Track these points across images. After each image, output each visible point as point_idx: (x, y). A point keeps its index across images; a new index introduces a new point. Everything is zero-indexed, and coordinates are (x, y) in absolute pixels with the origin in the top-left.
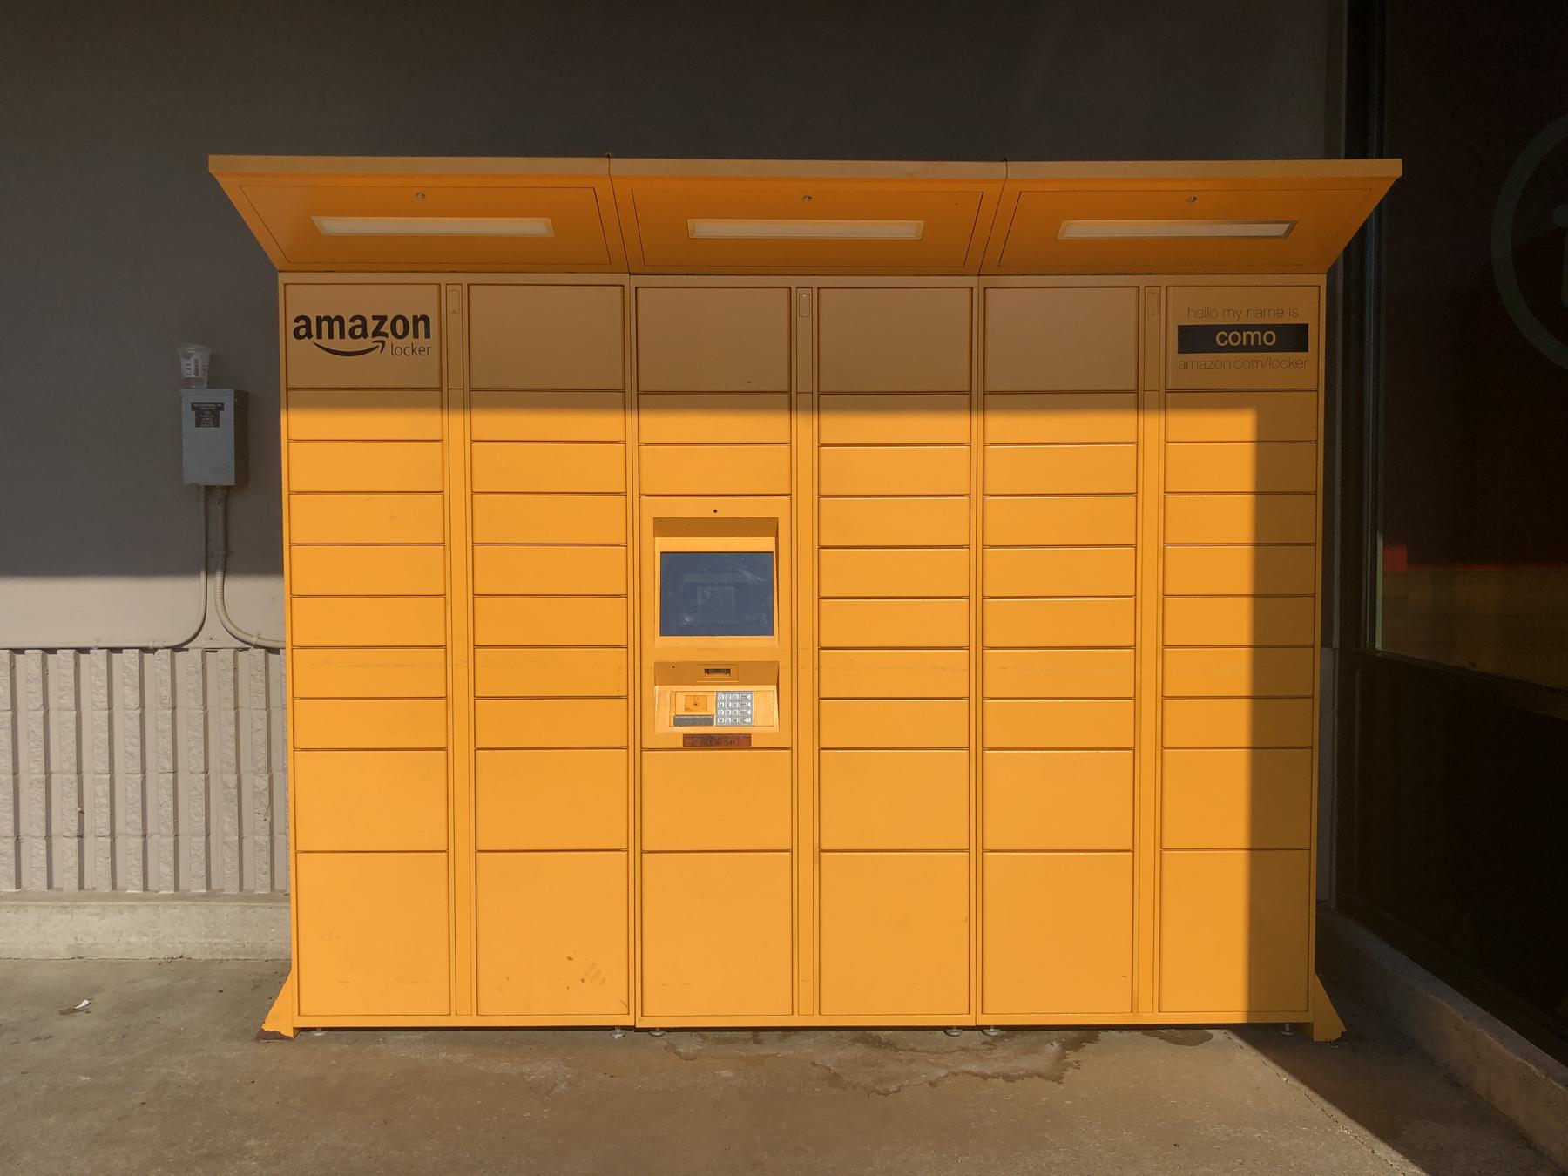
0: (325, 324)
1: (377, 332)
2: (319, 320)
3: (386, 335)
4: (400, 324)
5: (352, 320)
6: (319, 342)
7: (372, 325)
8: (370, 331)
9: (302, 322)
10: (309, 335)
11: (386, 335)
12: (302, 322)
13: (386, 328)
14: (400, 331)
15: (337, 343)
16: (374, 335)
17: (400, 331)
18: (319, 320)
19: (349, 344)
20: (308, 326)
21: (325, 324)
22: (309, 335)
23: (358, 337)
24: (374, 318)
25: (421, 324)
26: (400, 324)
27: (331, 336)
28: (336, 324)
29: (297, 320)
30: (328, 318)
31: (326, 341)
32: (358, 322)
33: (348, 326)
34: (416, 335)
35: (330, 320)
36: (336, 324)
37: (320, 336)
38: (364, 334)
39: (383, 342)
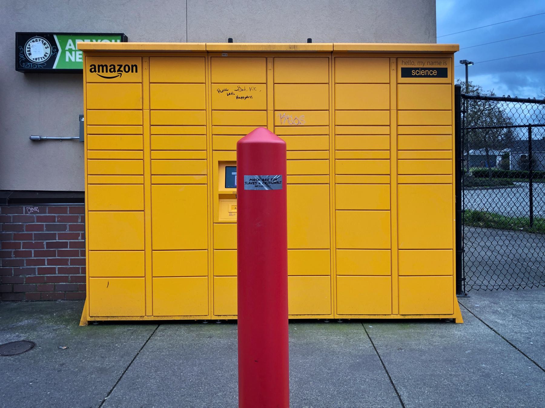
0: (101, 68)
1: (119, 70)
2: (99, 66)
3: (122, 71)
5: (110, 66)
6: (99, 74)
7: (117, 68)
8: (116, 70)
9: (93, 67)
10: (95, 71)
11: (122, 71)
12: (93, 67)
13: (122, 69)
14: (127, 70)
16: (118, 71)
17: (127, 70)
19: (109, 74)
20: (95, 68)
21: (101, 68)
22: (95, 71)
23: (112, 72)
25: (134, 68)
27: (103, 72)
28: (105, 68)
29: (91, 66)
30: (102, 65)
31: (101, 73)
32: (112, 67)
33: (109, 68)
34: (132, 72)
35: (103, 66)
36: (105, 68)
37: (99, 72)
38: (115, 71)
39: (121, 74)
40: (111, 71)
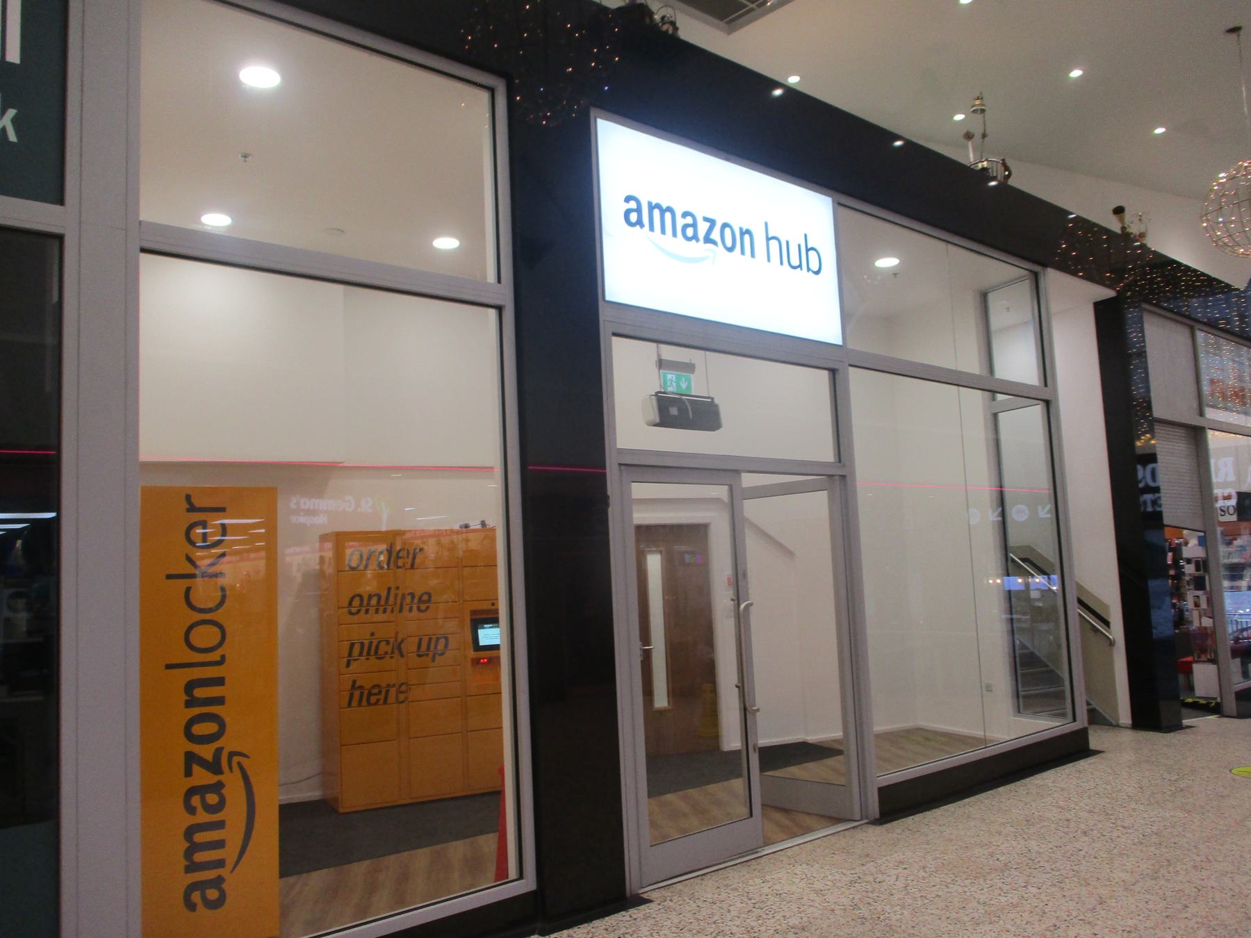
3: (219, 751)
4: (199, 729)
6: (230, 863)
8: (209, 778)
10: (218, 882)
11: (219, 751)
18: (192, 867)
21: (200, 857)
24: (188, 773)
25: (200, 693)
26: (199, 729)
27: (220, 844)
29: (191, 906)
30: (189, 854)
31: (229, 853)
37: (220, 863)
38: (217, 787)
39: (232, 755)
40: (221, 805)
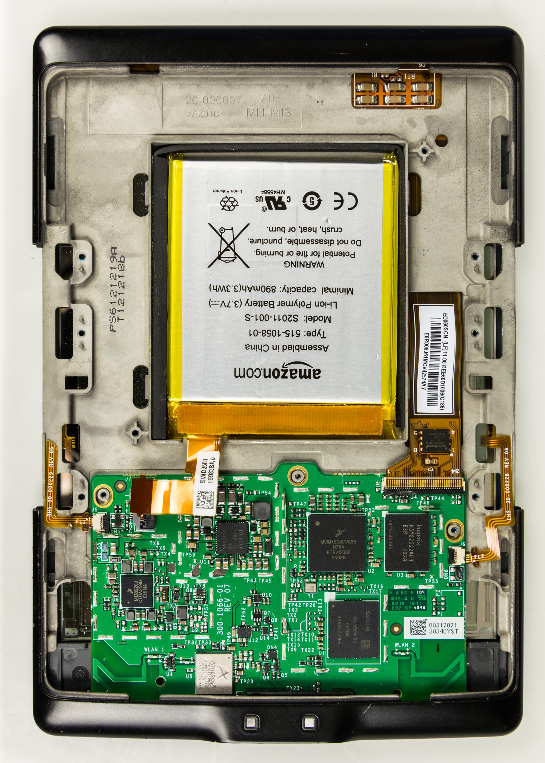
1: (286, 371)
3: (282, 370)
4: (276, 374)
5: (296, 377)
7: (288, 374)
9: (317, 376)
10: (314, 371)
12: (317, 376)
13: (282, 373)
15: (303, 367)
19: (298, 367)
20: (314, 374)
24: (287, 377)
26: (276, 374)
27: (305, 370)
28: (303, 374)
33: (298, 374)
36: (303, 374)
37: (310, 370)
38: (291, 370)
39: (283, 367)
40: (296, 370)
